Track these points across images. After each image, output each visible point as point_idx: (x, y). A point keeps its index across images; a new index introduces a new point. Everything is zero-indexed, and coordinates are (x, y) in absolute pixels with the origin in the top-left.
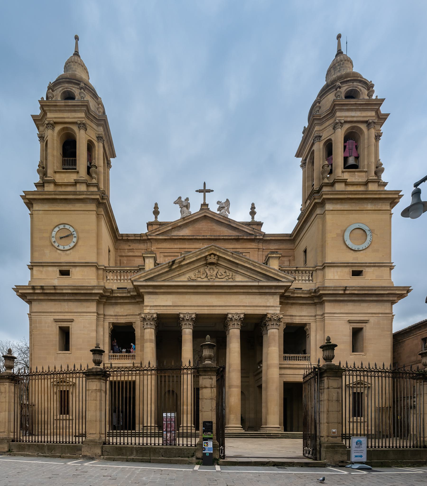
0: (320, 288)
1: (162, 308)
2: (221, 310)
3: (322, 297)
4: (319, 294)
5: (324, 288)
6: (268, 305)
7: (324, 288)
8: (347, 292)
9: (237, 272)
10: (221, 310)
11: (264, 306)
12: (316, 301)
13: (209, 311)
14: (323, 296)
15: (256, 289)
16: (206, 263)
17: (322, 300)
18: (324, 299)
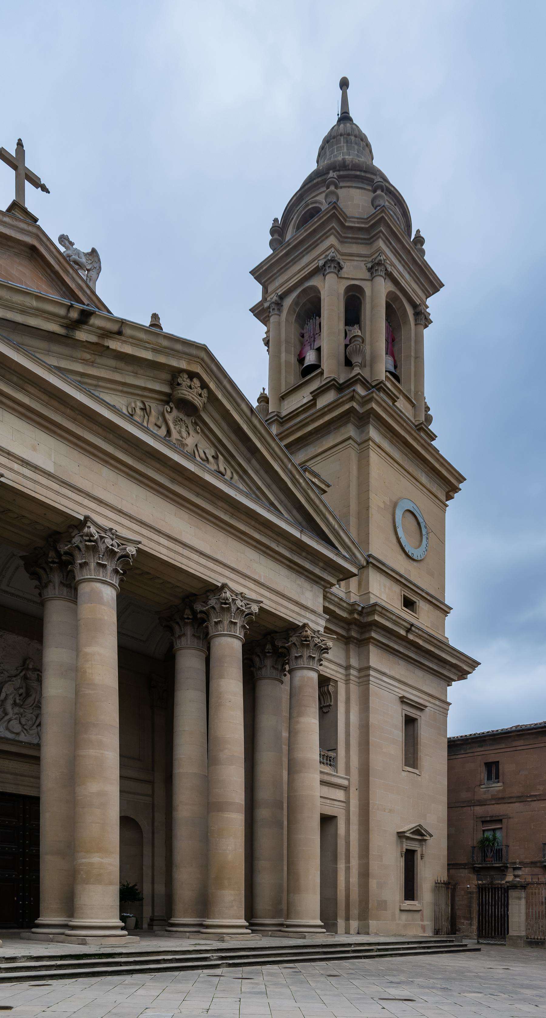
0: (377, 608)
1: (16, 467)
2: (205, 567)
3: (369, 631)
4: (370, 619)
5: (384, 612)
6: (304, 603)
7: (384, 612)
8: (411, 637)
9: (243, 473)
10: (205, 567)
11: (297, 603)
12: (354, 634)
13: (172, 555)
14: (374, 628)
15: (286, 547)
16: (169, 395)
17: (367, 636)
18: (373, 635)
